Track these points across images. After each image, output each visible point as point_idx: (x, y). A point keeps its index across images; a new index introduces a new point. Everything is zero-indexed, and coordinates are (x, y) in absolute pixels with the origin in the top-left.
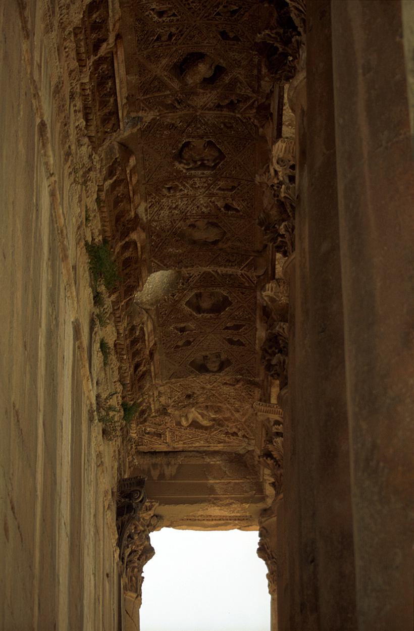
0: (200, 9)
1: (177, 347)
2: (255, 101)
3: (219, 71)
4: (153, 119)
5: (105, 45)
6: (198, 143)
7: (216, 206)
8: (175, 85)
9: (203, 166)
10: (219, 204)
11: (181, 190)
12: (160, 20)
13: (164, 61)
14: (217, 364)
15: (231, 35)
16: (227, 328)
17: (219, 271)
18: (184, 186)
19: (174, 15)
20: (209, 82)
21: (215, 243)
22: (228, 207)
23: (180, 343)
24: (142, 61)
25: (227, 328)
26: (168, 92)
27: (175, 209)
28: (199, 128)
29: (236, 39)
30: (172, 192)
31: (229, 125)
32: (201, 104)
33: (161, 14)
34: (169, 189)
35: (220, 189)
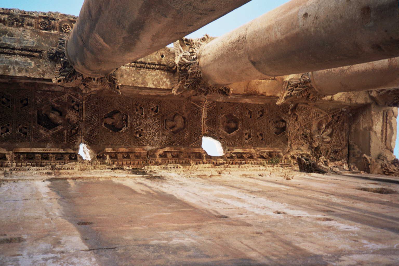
0: (5, 114)
1: (262, 139)
2: (71, 95)
3: (54, 109)
4: (84, 138)
5: (6, 155)
6: (110, 121)
7: (154, 116)
8: (60, 128)
9: (126, 120)
10: (153, 114)
11: (142, 130)
12: (10, 131)
13: (42, 131)
14: (281, 122)
15: (25, 102)
16: (251, 117)
17: (205, 118)
18: (137, 129)
19: (9, 125)
20: (62, 114)
21: (184, 118)
22: (156, 111)
23: (261, 138)
24: (38, 141)
25: (251, 117)
26: (65, 131)
27: (155, 134)
28: (95, 120)
29: (27, 99)
30: (142, 134)
31: (93, 107)
32: (76, 118)
33: (8, 131)
34: (140, 135)
35: (142, 114)
